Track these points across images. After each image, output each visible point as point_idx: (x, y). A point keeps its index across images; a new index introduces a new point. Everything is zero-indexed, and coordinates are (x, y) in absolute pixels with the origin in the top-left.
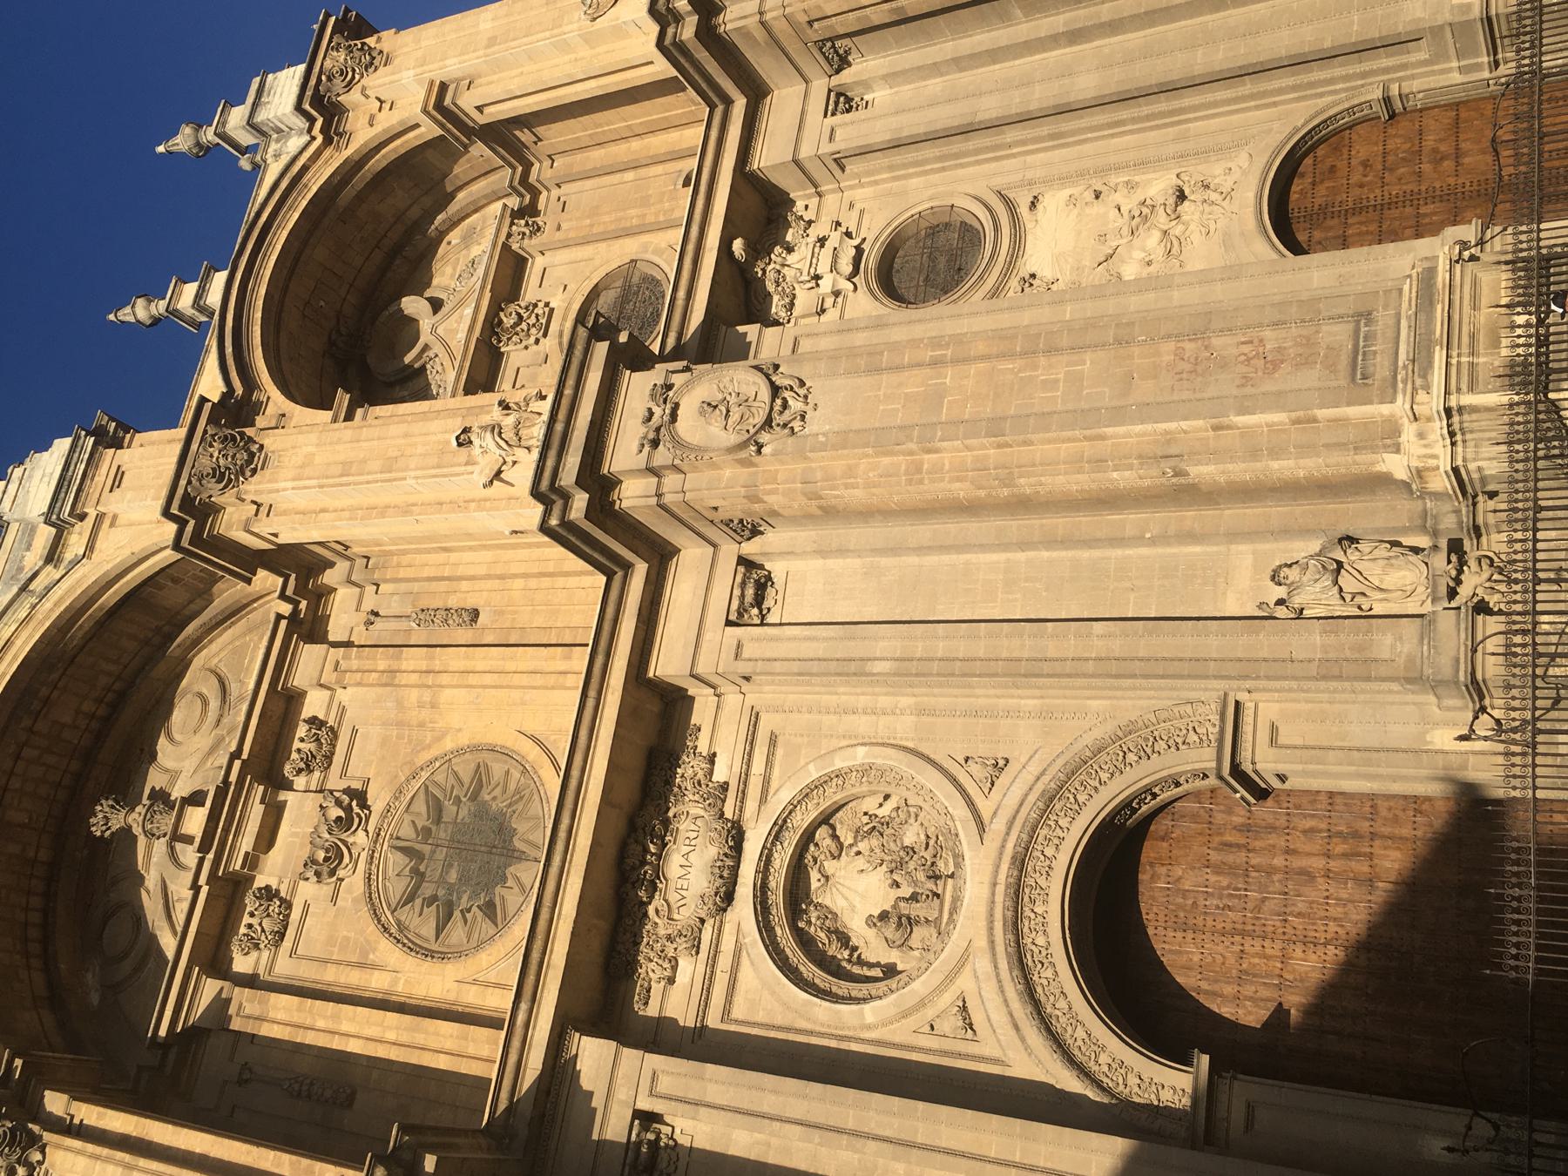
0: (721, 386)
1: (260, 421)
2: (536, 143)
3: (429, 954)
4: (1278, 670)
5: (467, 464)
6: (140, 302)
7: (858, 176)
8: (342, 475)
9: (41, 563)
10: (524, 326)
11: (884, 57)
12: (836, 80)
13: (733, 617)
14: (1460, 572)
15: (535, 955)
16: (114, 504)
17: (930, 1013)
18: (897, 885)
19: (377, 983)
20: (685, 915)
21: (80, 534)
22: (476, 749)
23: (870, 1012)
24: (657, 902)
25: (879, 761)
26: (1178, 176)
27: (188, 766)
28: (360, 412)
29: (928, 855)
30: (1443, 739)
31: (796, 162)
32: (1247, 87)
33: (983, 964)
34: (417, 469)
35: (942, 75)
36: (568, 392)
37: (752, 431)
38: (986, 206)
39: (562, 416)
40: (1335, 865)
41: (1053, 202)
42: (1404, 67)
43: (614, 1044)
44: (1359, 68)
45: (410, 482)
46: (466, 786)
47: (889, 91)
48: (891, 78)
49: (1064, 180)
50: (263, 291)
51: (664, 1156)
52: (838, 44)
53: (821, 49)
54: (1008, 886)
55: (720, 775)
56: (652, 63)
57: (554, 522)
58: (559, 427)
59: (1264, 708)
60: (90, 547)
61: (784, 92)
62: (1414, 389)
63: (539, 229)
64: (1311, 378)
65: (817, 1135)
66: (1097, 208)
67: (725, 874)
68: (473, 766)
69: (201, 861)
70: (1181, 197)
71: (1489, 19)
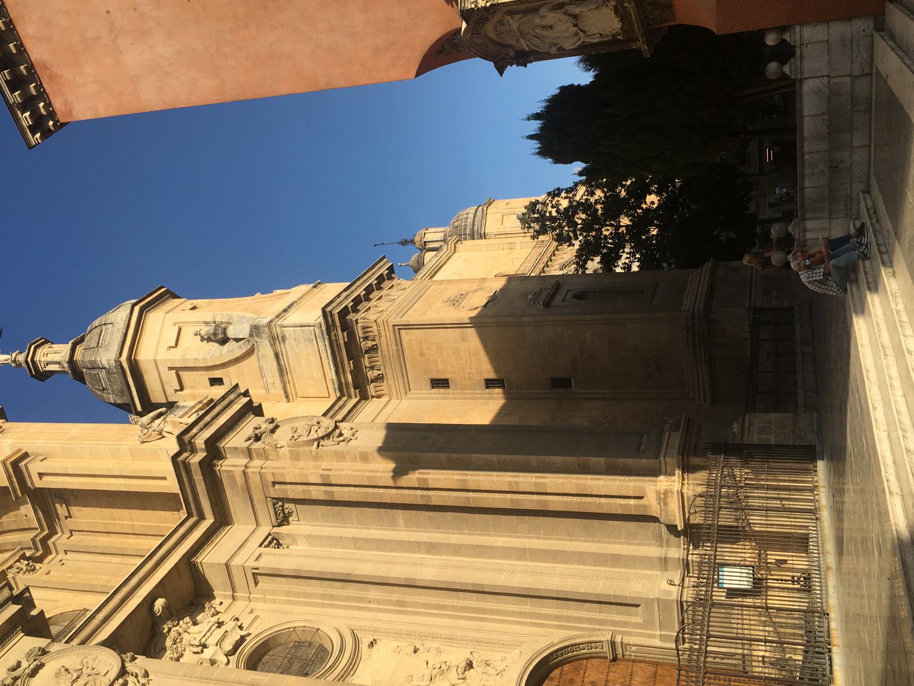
0: (84, 662)
2: (66, 518)
7: (264, 592)
11: (311, 525)
12: (276, 530)
26: (471, 653)
31: (227, 566)
32: (528, 606)
35: (343, 548)
42: (626, 624)
44: (598, 616)
47: (307, 548)
48: (311, 538)
49: (398, 635)
52: (286, 506)
53: (274, 504)
56: (165, 478)
61: (241, 526)
63: (34, 569)
70: (470, 665)
71: (681, 603)
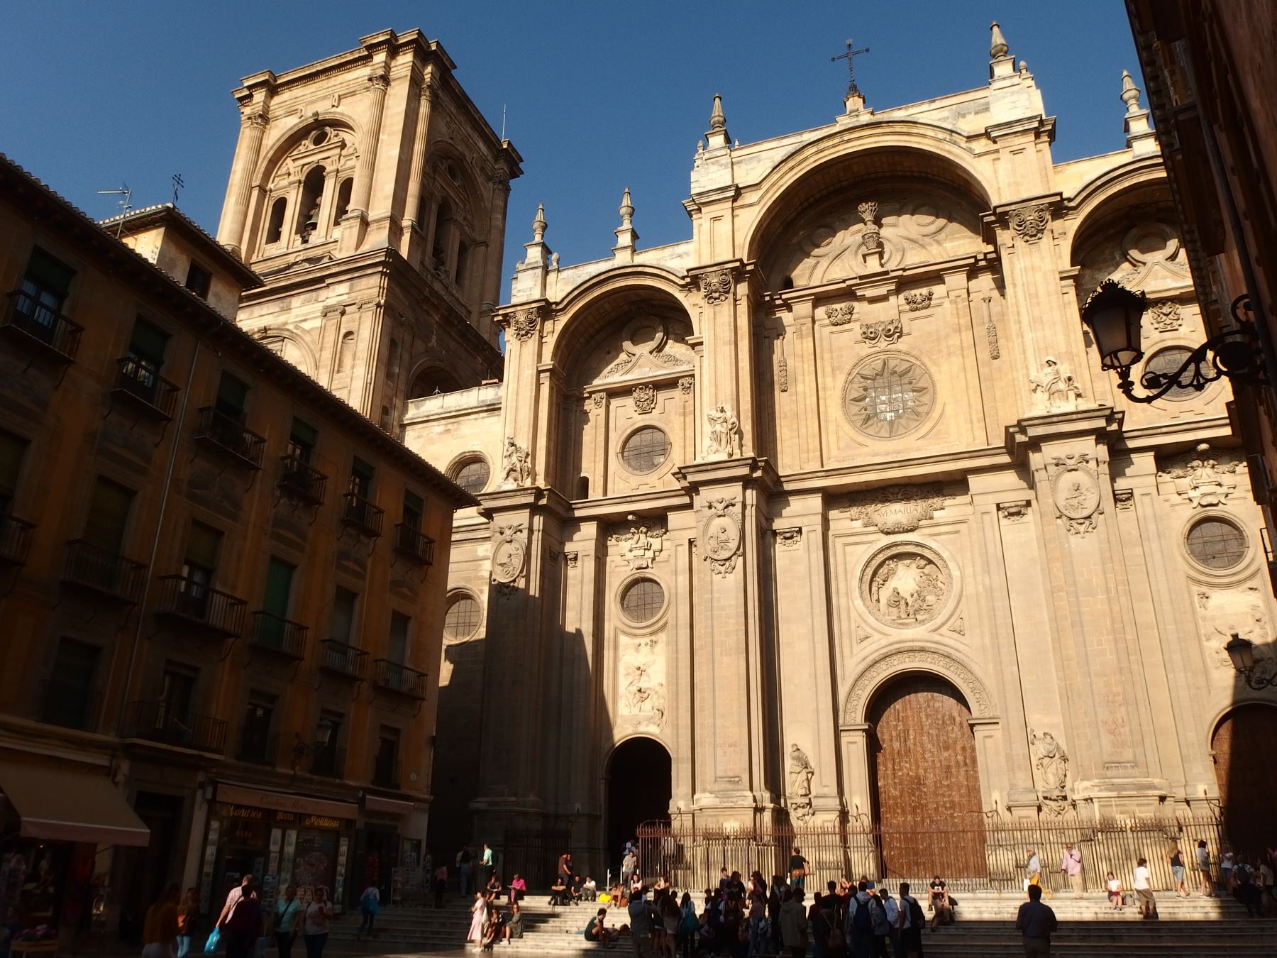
1: (1058, 223)
3: (844, 398)
4: (1008, 739)
5: (1042, 365)
6: (1133, 93)
8: (1030, 295)
9: (966, 134)
10: (1164, 318)
13: (1001, 506)
14: (1055, 800)
15: (842, 471)
16: (1005, 155)
17: (863, 625)
18: (912, 595)
19: (829, 381)
20: (877, 518)
21: (986, 145)
22: (933, 382)
23: (858, 602)
24: (880, 505)
25: (954, 582)
27: (901, 231)
28: (1071, 281)
29: (925, 607)
30: (996, 795)
33: (884, 642)
34: (1036, 337)
36: (1074, 417)
37: (1066, 513)
38: (1251, 562)
39: (1061, 418)
40: (953, 758)
41: (1255, 598)
43: (821, 511)
45: (1030, 335)
46: (917, 386)
50: (1143, 178)
51: (790, 541)
54: (912, 647)
55: (937, 514)
57: (1011, 430)
58: (1055, 419)
59: (997, 732)
60: (980, 155)
62: (1099, 786)
64: (1107, 746)
65: (808, 600)
66: (1251, 621)
67: (897, 530)
68: (925, 386)
69: (856, 278)
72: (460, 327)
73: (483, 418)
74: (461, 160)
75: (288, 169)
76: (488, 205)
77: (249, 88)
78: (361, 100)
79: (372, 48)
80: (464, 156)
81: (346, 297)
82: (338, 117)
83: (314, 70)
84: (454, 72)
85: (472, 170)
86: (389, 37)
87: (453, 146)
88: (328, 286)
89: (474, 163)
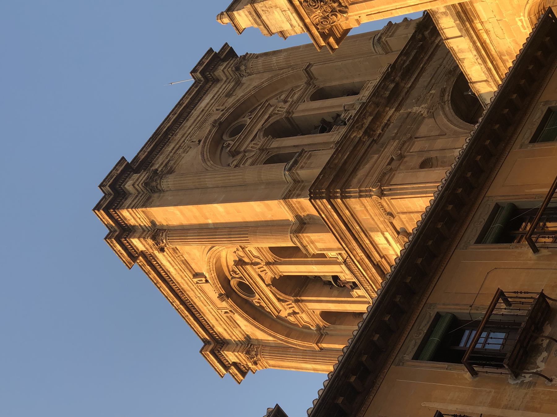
72: (397, 79)
73: (482, 23)
74: (220, 124)
75: (289, 315)
76: (267, 76)
77: (226, 368)
78: (188, 253)
79: (133, 255)
80: (215, 121)
81: (387, 235)
82: (214, 275)
83: (181, 306)
84: (129, 160)
85: (229, 108)
86: (113, 240)
87: (207, 138)
88: (383, 257)
89: (223, 107)
